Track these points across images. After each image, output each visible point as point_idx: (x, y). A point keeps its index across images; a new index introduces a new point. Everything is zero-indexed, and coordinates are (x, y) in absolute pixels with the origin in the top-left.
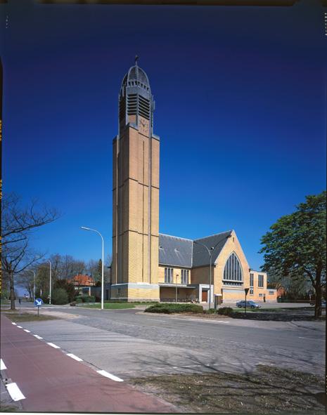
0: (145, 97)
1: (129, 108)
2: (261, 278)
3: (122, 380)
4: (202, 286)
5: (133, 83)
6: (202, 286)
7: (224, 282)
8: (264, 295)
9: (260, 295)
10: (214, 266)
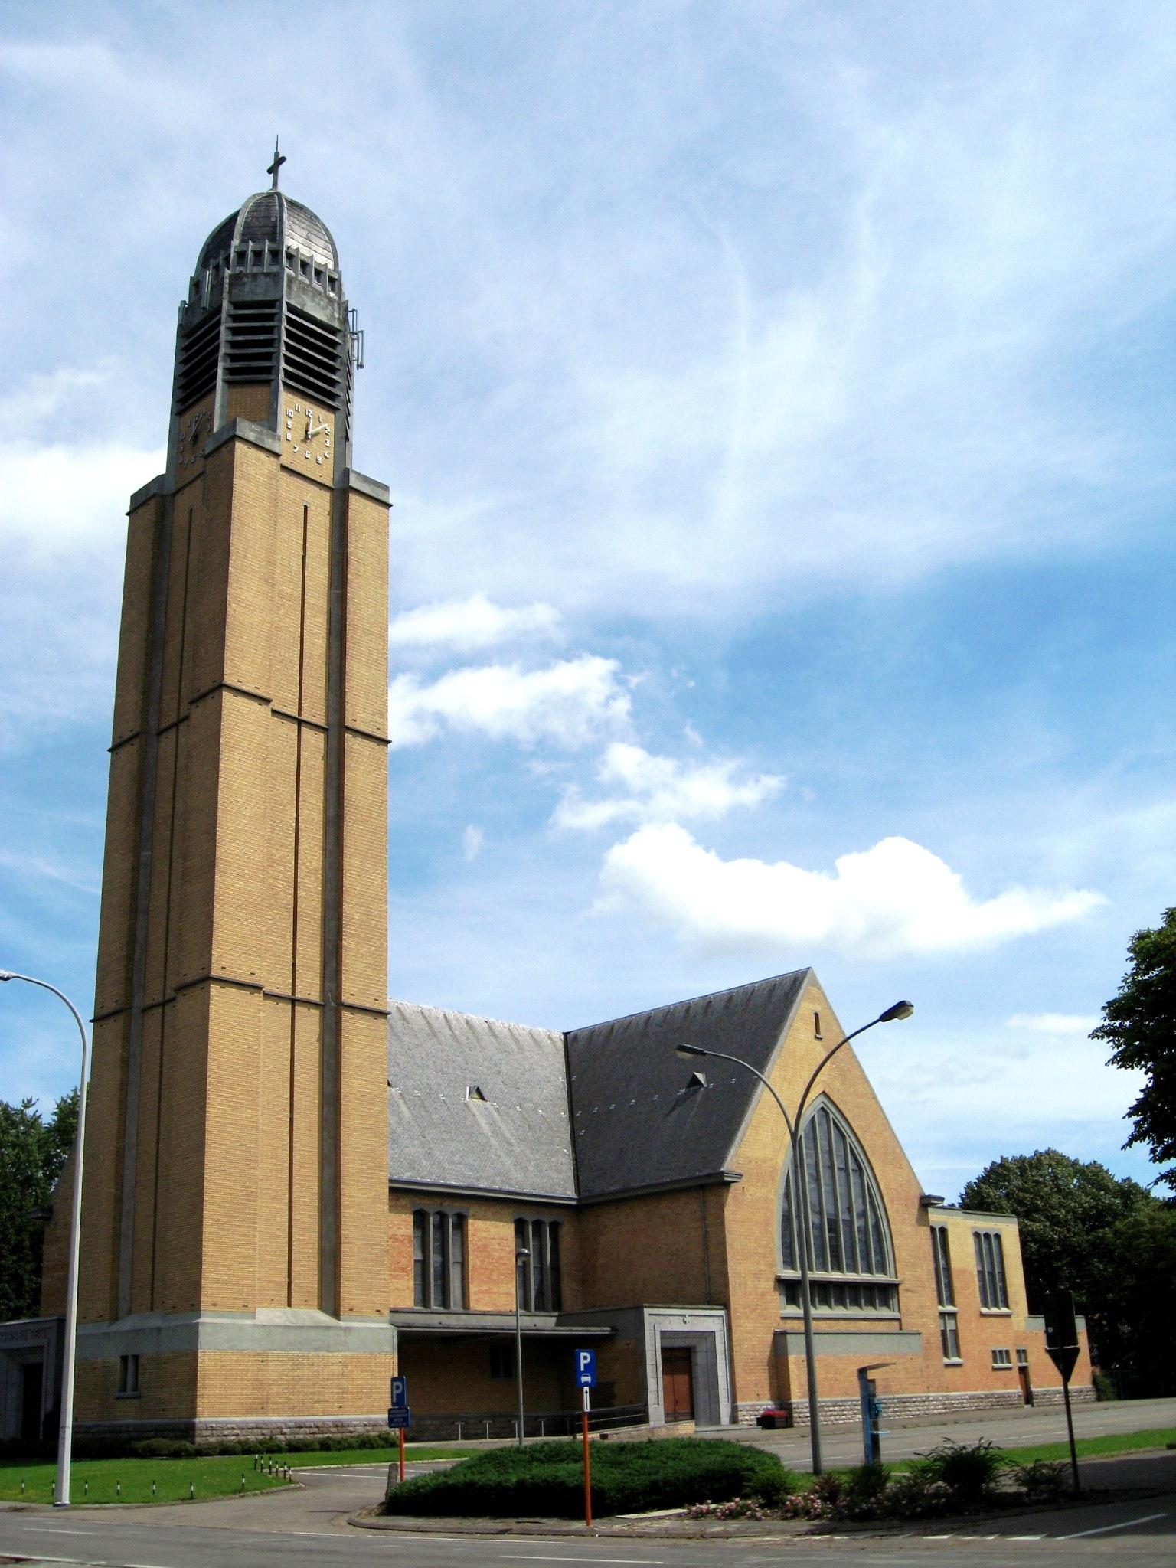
0: (321, 316)
1: (235, 318)
2: (988, 1243)
3: (215, 430)
4: (662, 1323)
5: (258, 255)
6: (662, 1323)
7: (790, 1290)
8: (1022, 1353)
9: (999, 1355)
10: (717, 1184)
